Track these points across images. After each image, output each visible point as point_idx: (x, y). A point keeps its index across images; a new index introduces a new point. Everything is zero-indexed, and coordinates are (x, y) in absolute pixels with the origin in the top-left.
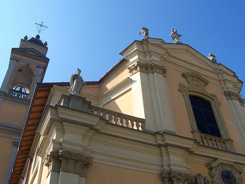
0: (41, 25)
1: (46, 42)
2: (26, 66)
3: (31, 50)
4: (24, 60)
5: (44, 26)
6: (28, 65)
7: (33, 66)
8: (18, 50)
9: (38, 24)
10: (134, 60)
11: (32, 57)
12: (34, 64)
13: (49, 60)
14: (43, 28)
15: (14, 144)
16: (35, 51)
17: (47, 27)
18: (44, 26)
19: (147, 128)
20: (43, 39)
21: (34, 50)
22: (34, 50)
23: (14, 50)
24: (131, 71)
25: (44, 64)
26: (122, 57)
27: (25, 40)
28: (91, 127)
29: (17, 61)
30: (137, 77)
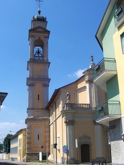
0: (39, 1)
1: (46, 17)
2: (38, 39)
3: (39, 27)
4: (37, 35)
5: (41, 1)
6: (39, 38)
7: (42, 38)
8: (32, 30)
9: (37, 1)
10: (87, 78)
11: (40, 33)
12: (42, 36)
13: (50, 32)
14: (41, 3)
15: (43, 86)
16: (42, 28)
17: (43, 1)
18: (41, 1)
19: (90, 107)
20: (42, 15)
21: (41, 27)
22: (41, 27)
23: (29, 30)
24: (86, 82)
25: (48, 35)
26: (83, 75)
27: (34, 20)
28: (74, 113)
29: (34, 37)
30: (87, 86)
